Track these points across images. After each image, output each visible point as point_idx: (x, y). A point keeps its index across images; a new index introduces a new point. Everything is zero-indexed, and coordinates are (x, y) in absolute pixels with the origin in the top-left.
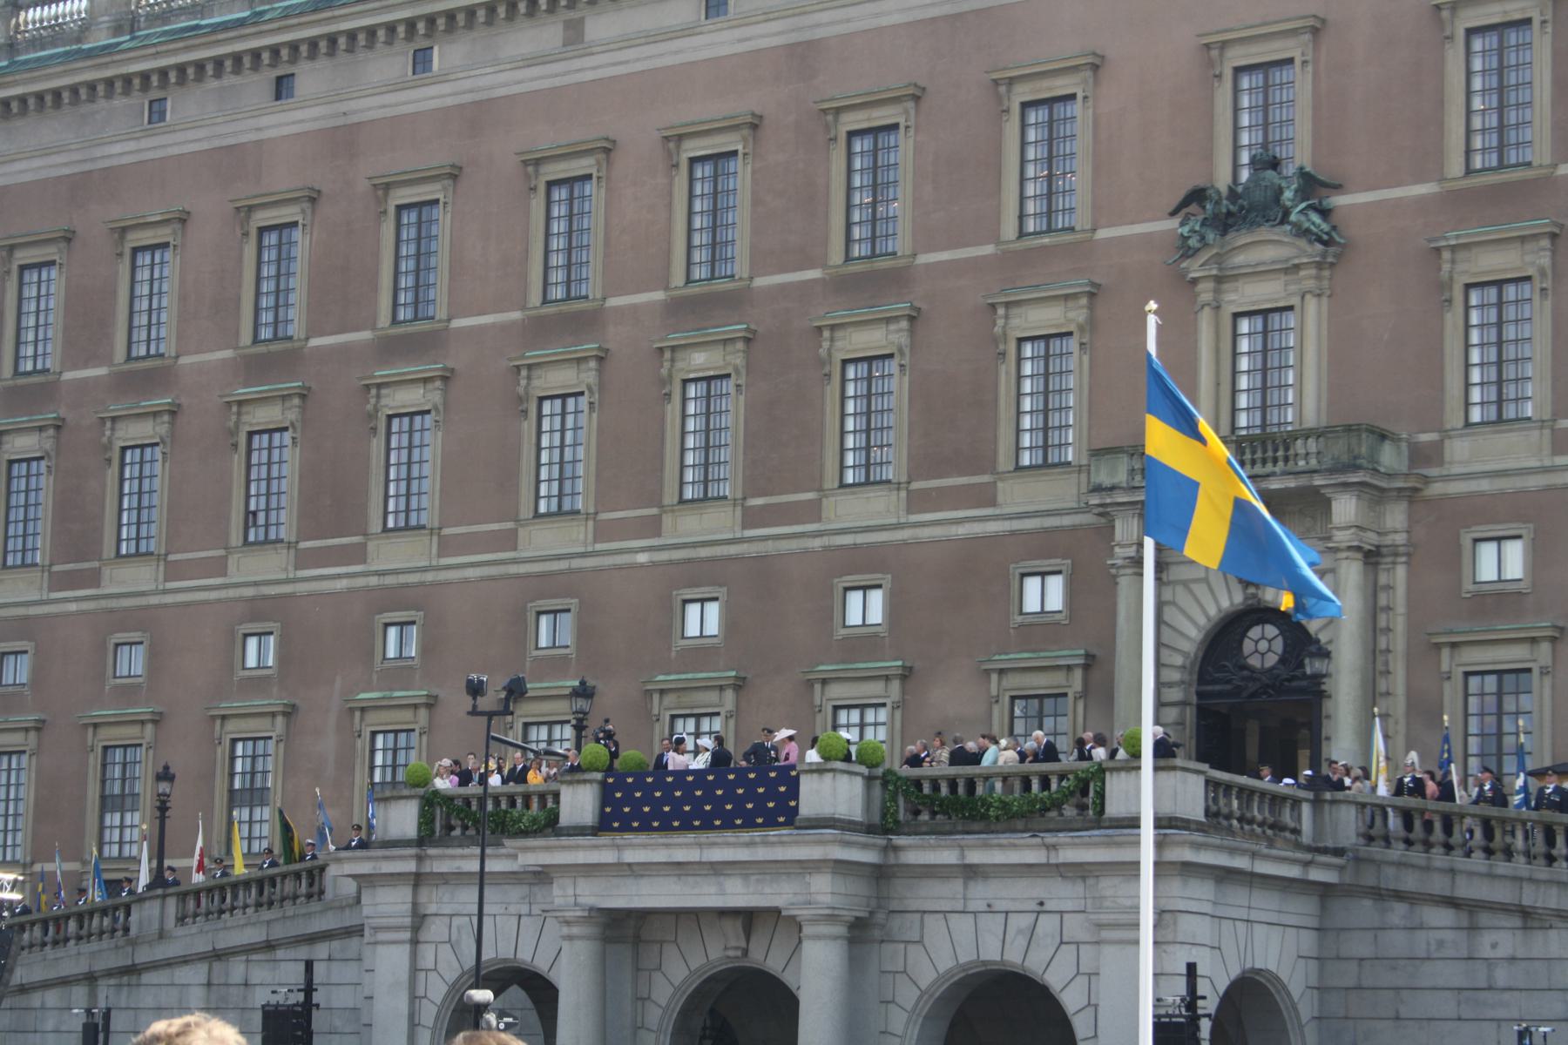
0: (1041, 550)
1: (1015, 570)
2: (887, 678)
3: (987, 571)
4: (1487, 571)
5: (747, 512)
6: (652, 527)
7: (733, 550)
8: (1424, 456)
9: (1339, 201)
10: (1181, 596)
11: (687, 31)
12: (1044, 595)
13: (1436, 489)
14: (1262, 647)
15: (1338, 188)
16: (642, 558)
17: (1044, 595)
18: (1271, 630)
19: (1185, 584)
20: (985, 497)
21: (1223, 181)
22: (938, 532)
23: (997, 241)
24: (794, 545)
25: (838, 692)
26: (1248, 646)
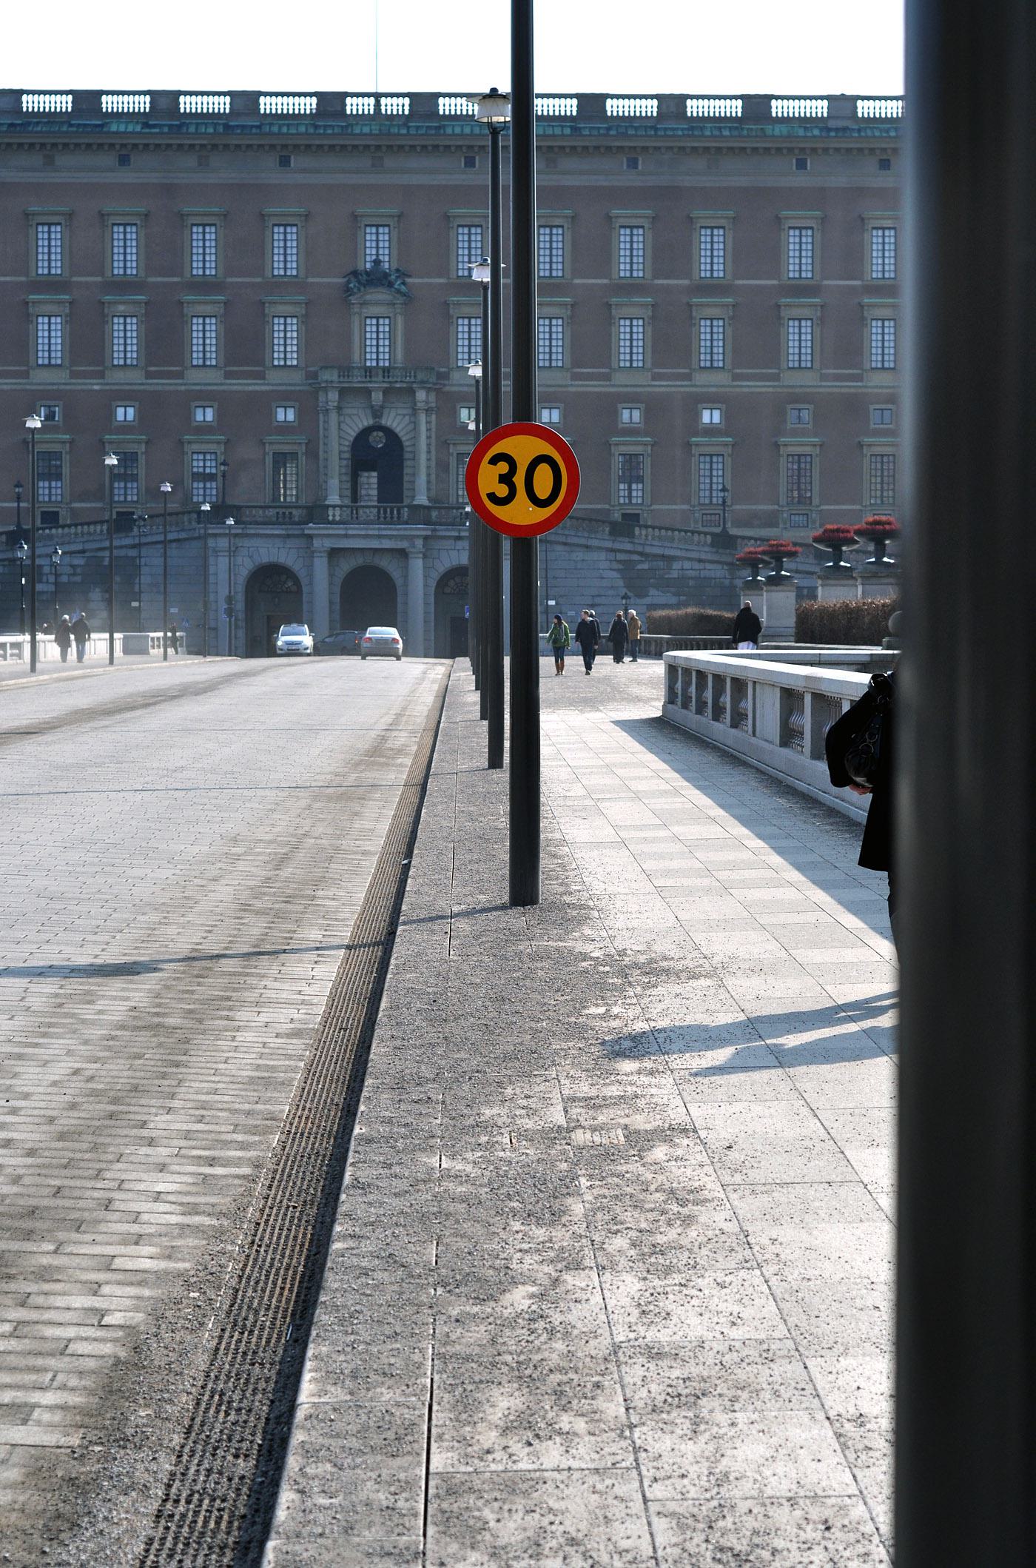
0: (285, 398)
1: (274, 405)
2: (219, 443)
3: (262, 404)
4: (199, 417)
5: (147, 372)
6: (101, 375)
7: (142, 387)
8: (445, 376)
9: (408, 280)
10: (348, 420)
11: (112, 170)
12: (286, 415)
13: (447, 389)
14: (378, 440)
15: (410, 276)
16: (96, 387)
17: (286, 415)
18: (381, 434)
19: (350, 416)
20: (261, 376)
21: (361, 267)
22: (239, 388)
23: (263, 276)
24: (172, 388)
25: (195, 447)
26: (371, 439)
